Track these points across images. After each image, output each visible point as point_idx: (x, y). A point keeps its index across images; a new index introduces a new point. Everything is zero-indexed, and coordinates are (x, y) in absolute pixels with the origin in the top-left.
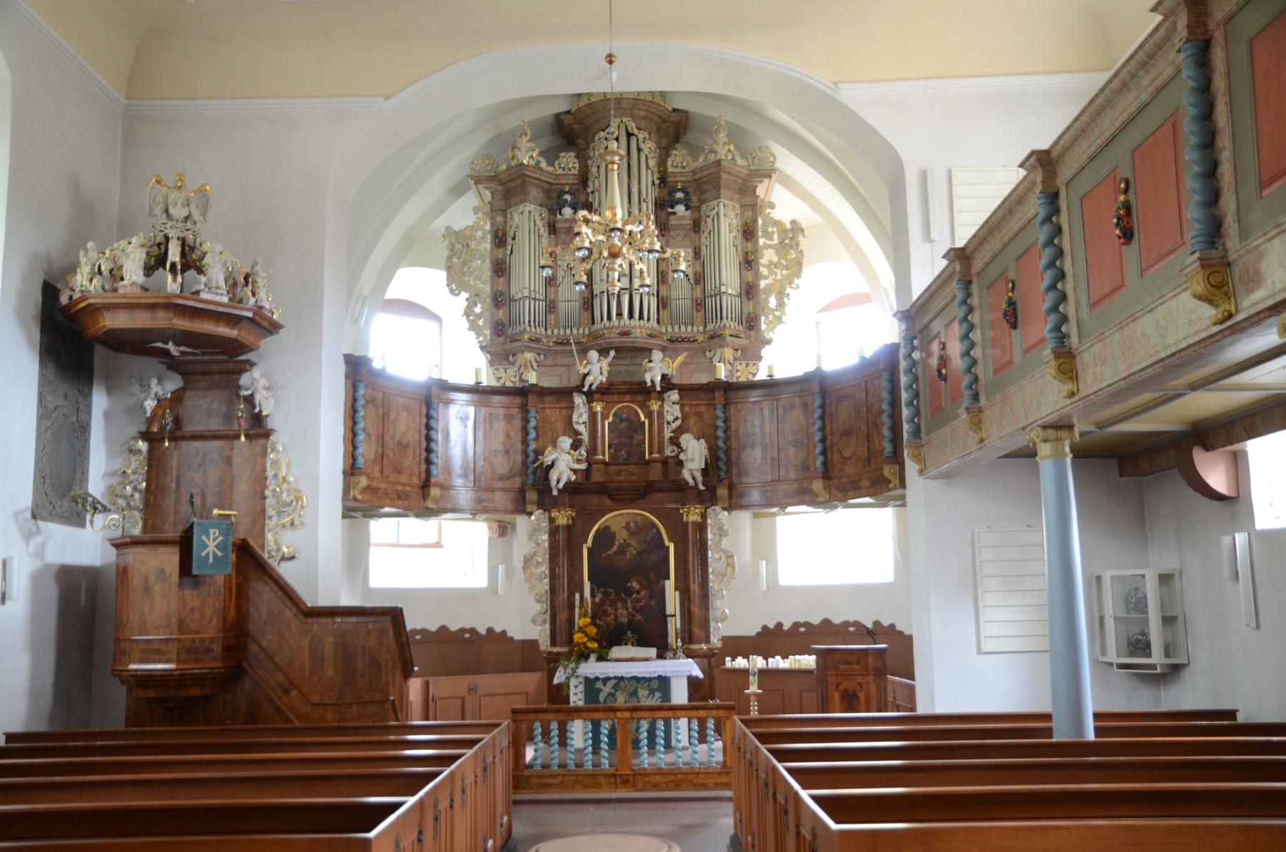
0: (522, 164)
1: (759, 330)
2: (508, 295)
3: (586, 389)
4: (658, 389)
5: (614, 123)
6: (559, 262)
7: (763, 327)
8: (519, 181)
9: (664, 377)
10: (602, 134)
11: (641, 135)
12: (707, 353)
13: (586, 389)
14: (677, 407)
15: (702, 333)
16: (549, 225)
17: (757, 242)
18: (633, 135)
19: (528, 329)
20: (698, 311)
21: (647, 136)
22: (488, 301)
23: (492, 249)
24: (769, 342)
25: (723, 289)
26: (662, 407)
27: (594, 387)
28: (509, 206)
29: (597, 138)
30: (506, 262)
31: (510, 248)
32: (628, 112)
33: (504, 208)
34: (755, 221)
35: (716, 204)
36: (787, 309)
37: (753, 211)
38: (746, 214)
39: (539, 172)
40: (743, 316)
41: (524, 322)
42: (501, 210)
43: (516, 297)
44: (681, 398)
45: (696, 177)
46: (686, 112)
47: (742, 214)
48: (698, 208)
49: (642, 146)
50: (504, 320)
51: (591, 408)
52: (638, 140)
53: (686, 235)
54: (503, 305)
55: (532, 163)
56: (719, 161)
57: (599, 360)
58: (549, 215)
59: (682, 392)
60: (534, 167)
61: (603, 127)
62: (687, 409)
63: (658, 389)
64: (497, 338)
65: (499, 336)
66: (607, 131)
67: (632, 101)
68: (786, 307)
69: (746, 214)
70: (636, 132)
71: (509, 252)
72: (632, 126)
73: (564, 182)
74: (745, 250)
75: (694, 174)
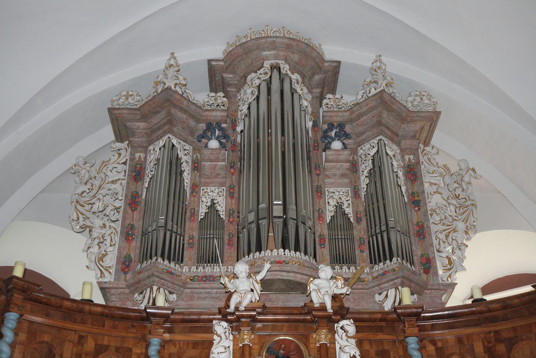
0: (169, 88)
1: (436, 274)
2: (140, 230)
3: (232, 309)
4: (330, 310)
5: (267, 64)
6: (204, 199)
7: (440, 272)
8: (163, 114)
9: (335, 298)
10: (253, 75)
11: (295, 77)
12: (377, 296)
13: (232, 309)
14: (353, 341)
15: (368, 274)
16: (194, 162)
17: (422, 184)
18: (287, 75)
19: (160, 260)
20: (362, 251)
21: (300, 80)
22: (117, 239)
23: (128, 183)
24: (453, 286)
25: (391, 224)
26: (333, 341)
27: (242, 308)
28: (151, 142)
29: (249, 78)
30: (142, 195)
31: (148, 180)
32: (282, 53)
33: (145, 145)
34: (418, 163)
35: (376, 142)
36: (468, 252)
37: (414, 155)
38: (407, 157)
39: (185, 102)
40: (415, 258)
41: (156, 255)
42: (142, 147)
43: (150, 230)
44: (357, 332)
45: (353, 116)
46: (339, 62)
47: (403, 157)
48: (354, 152)
49: (298, 88)
50: (132, 255)
51: (235, 340)
52: (291, 81)
53: (343, 176)
54: (133, 239)
55: (178, 89)
56: (383, 91)
57: (249, 276)
58: (194, 152)
59: (359, 324)
60: (182, 96)
61: (256, 69)
62: (367, 347)
63: (330, 310)
64: (123, 276)
65: (126, 273)
66: (259, 72)
67: (286, 41)
68: (467, 250)
69: (407, 157)
70: (289, 72)
71: (146, 185)
72: (285, 68)
73: (213, 118)
74: (410, 192)
75: (352, 114)
